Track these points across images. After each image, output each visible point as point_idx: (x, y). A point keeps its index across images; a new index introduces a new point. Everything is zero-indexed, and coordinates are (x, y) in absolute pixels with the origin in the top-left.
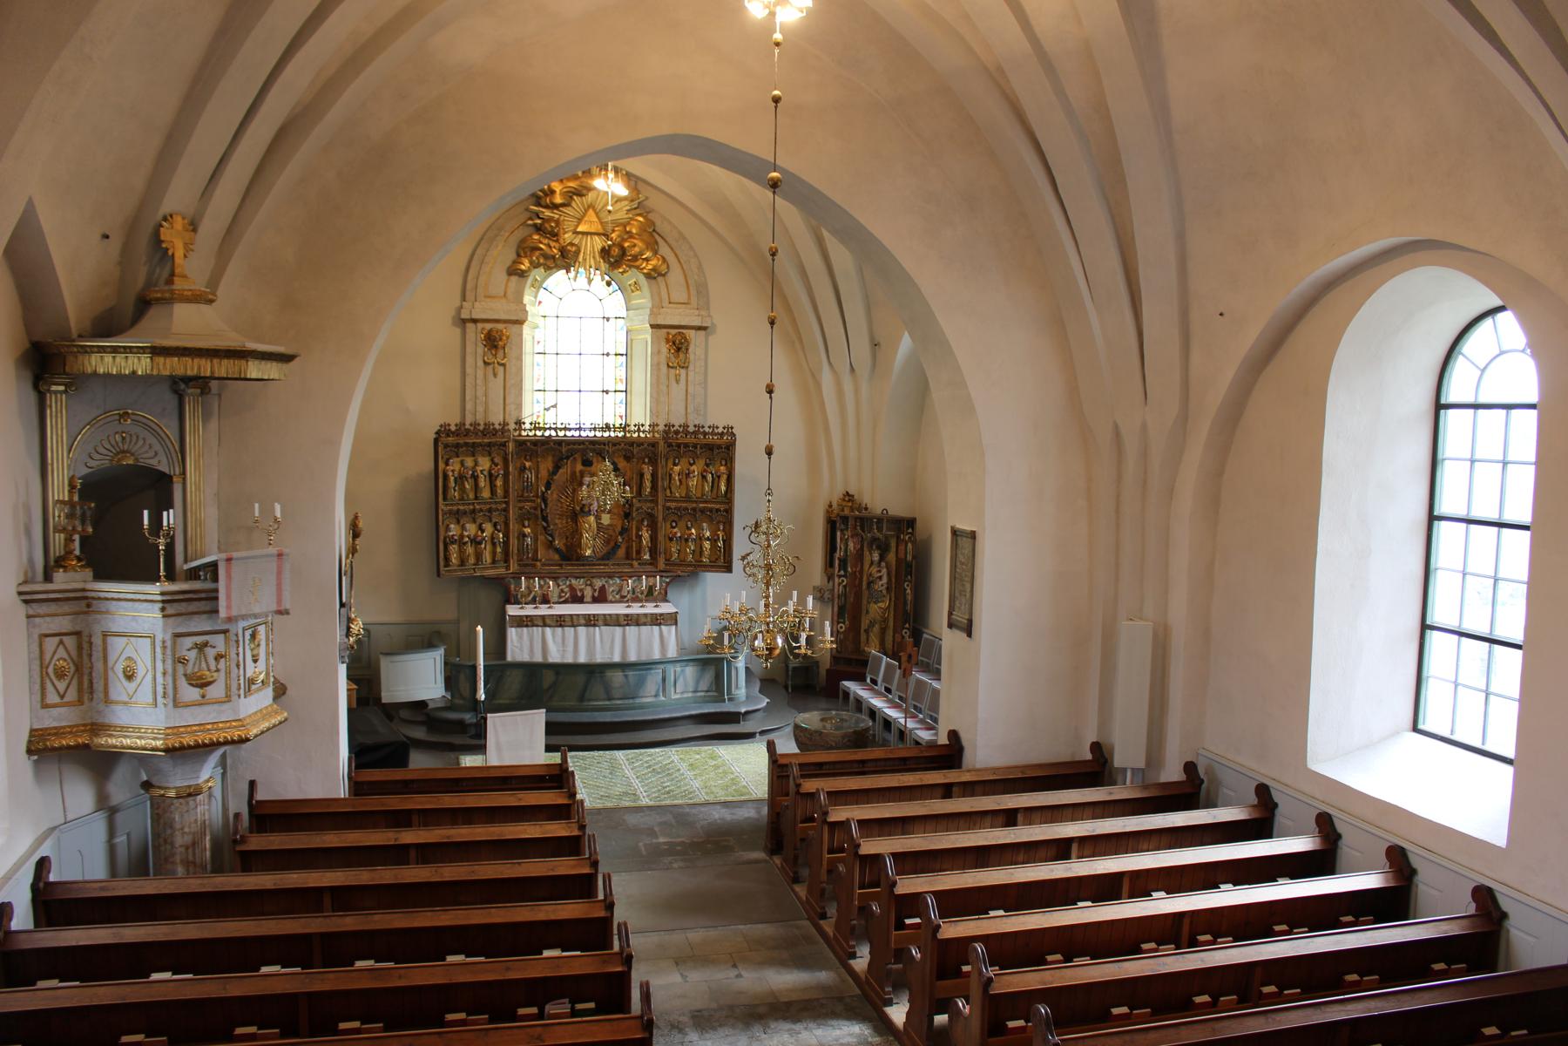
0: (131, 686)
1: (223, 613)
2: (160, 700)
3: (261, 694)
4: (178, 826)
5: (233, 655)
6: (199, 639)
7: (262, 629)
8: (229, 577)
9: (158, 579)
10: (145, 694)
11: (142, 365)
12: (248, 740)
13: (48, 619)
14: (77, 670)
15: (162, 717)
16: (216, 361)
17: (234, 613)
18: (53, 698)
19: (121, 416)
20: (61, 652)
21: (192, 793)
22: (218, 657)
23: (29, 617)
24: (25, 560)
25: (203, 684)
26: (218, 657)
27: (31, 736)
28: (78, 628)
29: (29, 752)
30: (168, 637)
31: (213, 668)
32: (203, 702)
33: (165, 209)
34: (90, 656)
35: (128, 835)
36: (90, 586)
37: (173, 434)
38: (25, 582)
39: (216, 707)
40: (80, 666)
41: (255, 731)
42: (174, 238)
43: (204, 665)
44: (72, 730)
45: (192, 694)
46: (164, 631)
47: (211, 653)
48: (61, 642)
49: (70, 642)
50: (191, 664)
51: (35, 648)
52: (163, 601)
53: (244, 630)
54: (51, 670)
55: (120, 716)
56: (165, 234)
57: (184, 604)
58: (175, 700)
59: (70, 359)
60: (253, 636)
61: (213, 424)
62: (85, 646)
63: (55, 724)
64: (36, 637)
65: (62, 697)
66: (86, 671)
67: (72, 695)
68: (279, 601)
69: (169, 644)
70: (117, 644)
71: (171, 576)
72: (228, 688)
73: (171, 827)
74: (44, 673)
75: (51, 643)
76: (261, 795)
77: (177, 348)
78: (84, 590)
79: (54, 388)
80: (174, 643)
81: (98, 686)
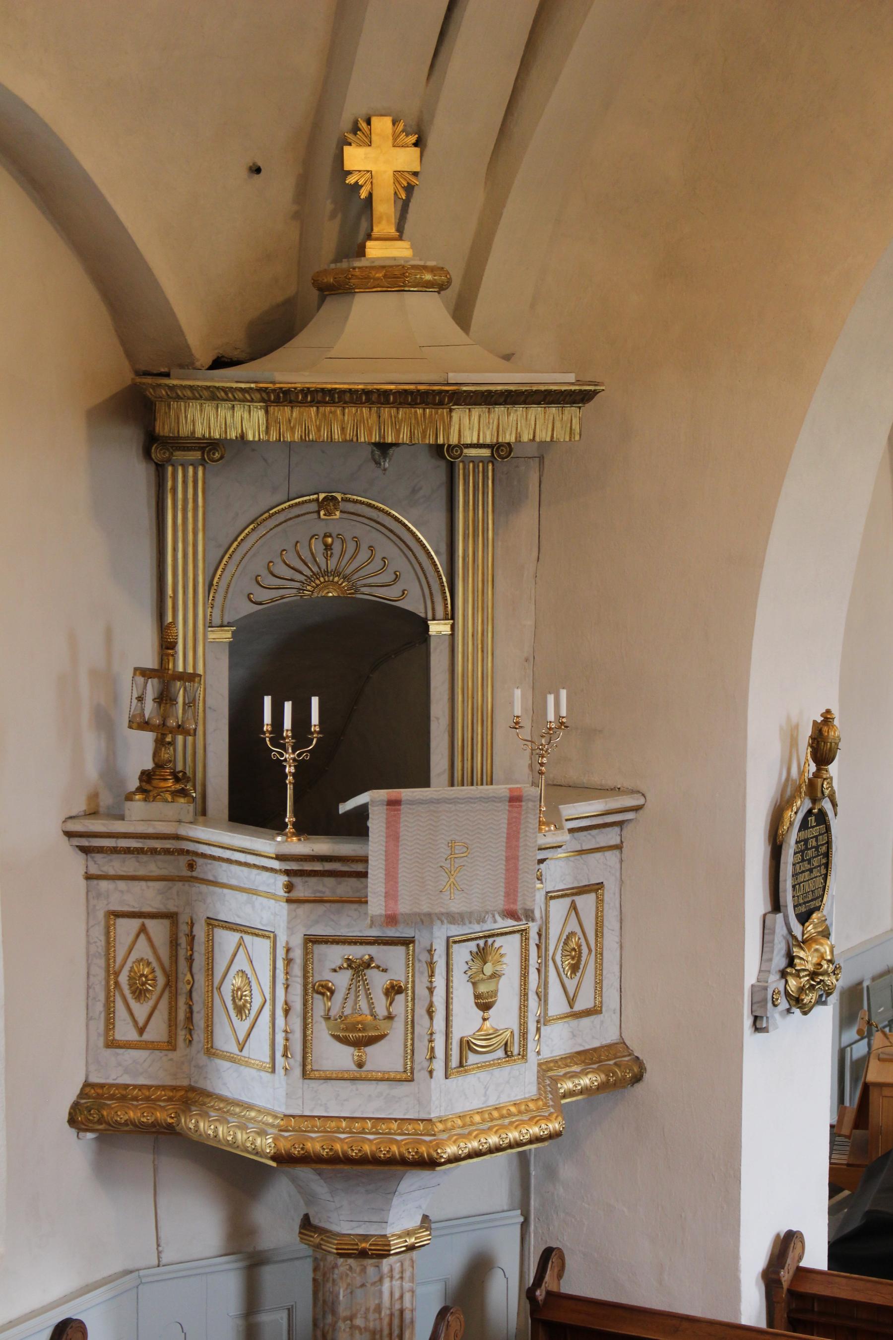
0: (242, 1027)
1: (376, 906)
2: (280, 1061)
3: (503, 1074)
4: (343, 1311)
5: (421, 991)
6: (359, 952)
7: (509, 947)
8: (393, 836)
9: (280, 827)
10: (259, 1048)
11: (249, 422)
12: (430, 1163)
13: (121, 884)
14: (168, 984)
15: (282, 1092)
16: (386, 412)
17: (403, 907)
18: (125, 1031)
19: (321, 504)
20: (142, 949)
21: (373, 1251)
22: (394, 990)
23: (89, 877)
24: (92, 770)
25: (360, 1037)
26: (394, 990)
27: (82, 1094)
28: (172, 908)
29: (72, 1121)
30: (297, 942)
31: (381, 1011)
32: (359, 1075)
33: (353, 108)
34: (190, 960)
35: (290, 1311)
36: (184, 831)
37: (430, 541)
38: (93, 814)
39: (383, 1087)
40: (171, 978)
41: (451, 1150)
42: (379, 161)
43: (363, 1004)
44: (145, 1095)
45: (340, 1057)
46: (291, 930)
47: (378, 981)
48: (143, 929)
49: (158, 929)
50: (339, 997)
51: (98, 933)
52: (287, 873)
53: (449, 943)
54: (123, 979)
55: (229, 1081)
56: (356, 158)
57: (330, 881)
58: (304, 1065)
59: (161, 408)
60: (482, 955)
61: (526, 519)
62: (183, 941)
63: (126, 1080)
64: (101, 915)
65: (141, 1031)
66: (184, 988)
67: (157, 1030)
68: (511, 892)
69: (297, 954)
70: (227, 940)
71: (304, 829)
72: (411, 1053)
73: (334, 1312)
74: (115, 985)
75: (127, 928)
76: (578, 1282)
77: (306, 392)
78: (177, 837)
79: (179, 455)
80: (306, 953)
81: (199, 1019)
